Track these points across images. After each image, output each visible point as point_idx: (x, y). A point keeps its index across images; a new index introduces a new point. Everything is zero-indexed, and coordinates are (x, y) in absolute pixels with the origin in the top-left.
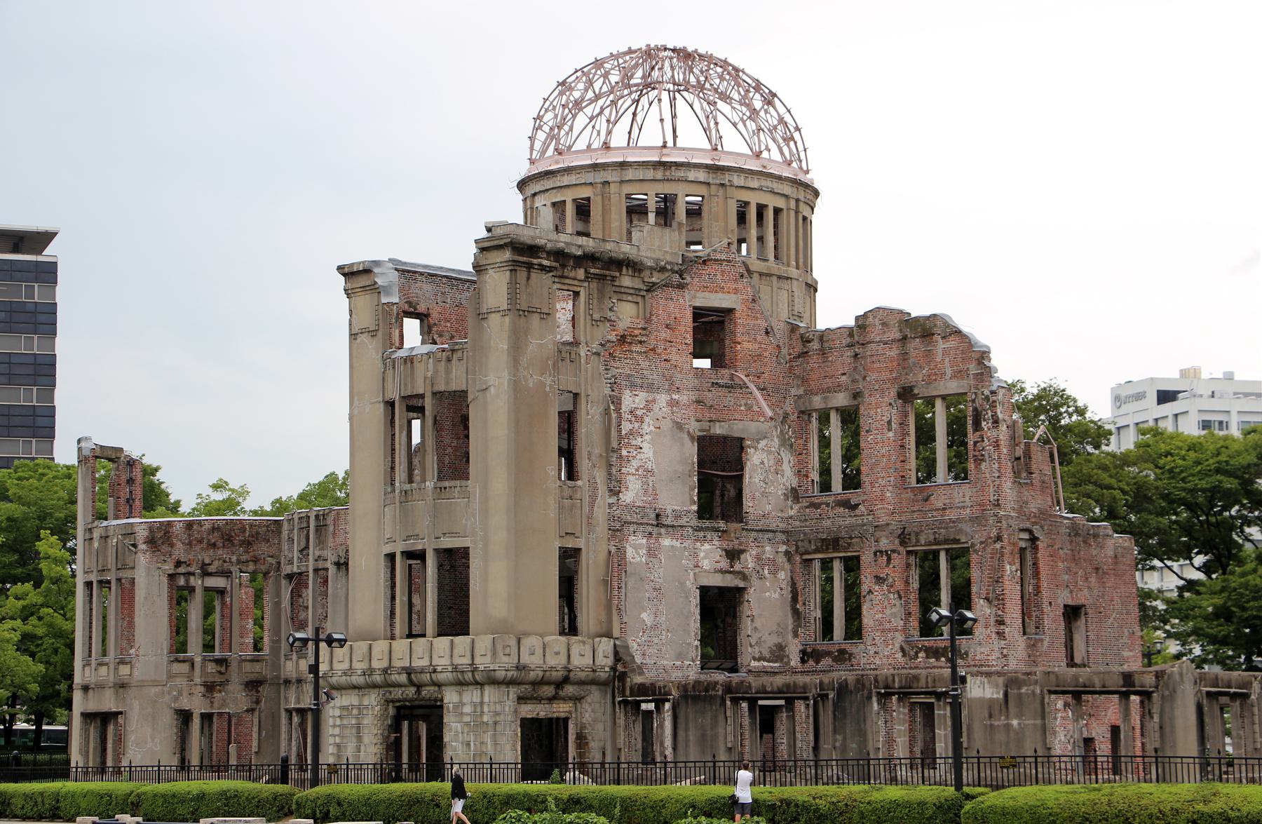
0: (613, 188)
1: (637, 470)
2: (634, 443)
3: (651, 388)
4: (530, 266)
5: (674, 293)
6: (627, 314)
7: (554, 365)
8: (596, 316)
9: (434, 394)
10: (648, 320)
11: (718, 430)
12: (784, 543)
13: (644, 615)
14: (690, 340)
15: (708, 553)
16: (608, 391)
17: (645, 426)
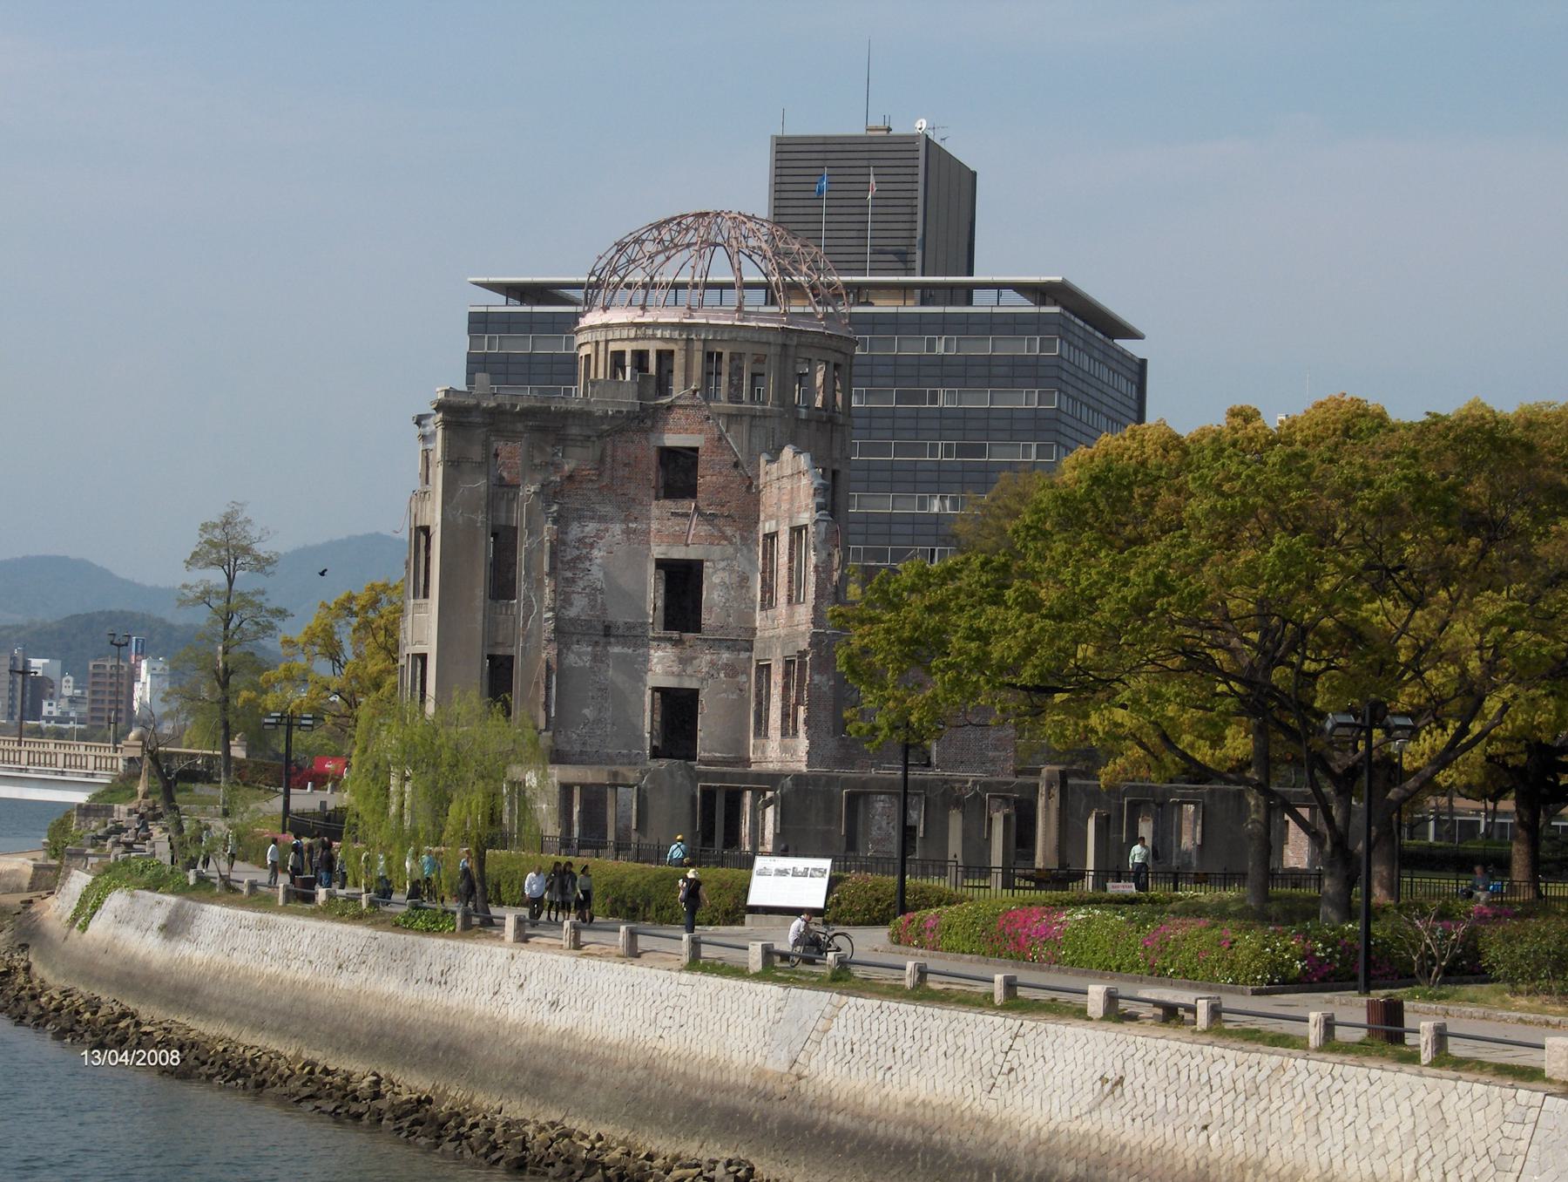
0: (602, 347)
1: (584, 589)
2: (581, 566)
3: (602, 519)
4: (461, 424)
5: (636, 438)
7: (488, 504)
8: (537, 461)
9: (416, 528)
10: (602, 461)
11: (678, 553)
12: (747, 650)
13: (586, 711)
14: (652, 476)
15: (661, 659)
16: (549, 525)
17: (595, 553)
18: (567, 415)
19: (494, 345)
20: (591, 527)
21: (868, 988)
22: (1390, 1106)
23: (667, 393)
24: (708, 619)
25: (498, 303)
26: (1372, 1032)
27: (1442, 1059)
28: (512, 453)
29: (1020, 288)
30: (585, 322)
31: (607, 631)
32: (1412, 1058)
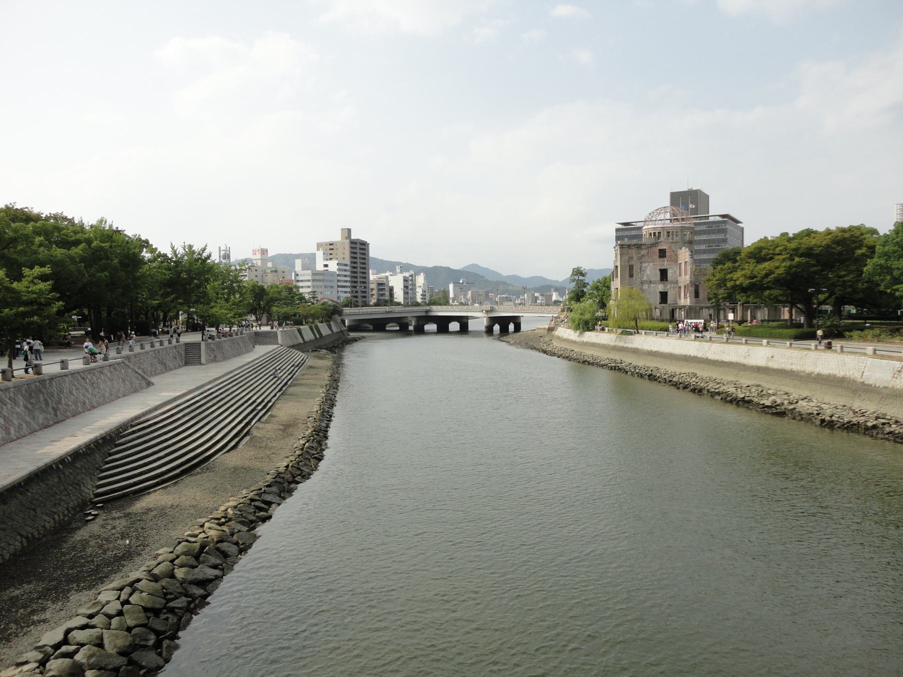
3: (649, 262)
6: (644, 252)
18: (641, 245)
19: (620, 234)
20: (647, 264)
21: (715, 342)
22: (832, 360)
23: (658, 239)
24: (669, 279)
25: (620, 226)
26: (826, 347)
27: (842, 351)
28: (633, 252)
29: (720, 216)
30: (644, 228)
31: (650, 282)
32: (836, 351)
